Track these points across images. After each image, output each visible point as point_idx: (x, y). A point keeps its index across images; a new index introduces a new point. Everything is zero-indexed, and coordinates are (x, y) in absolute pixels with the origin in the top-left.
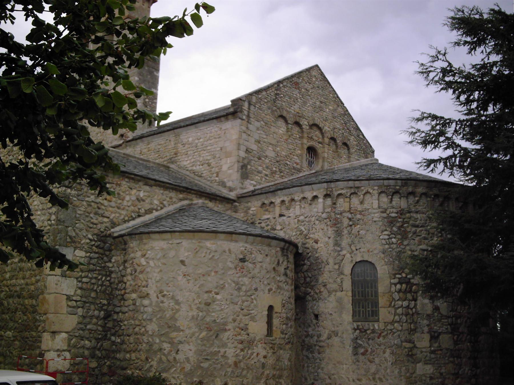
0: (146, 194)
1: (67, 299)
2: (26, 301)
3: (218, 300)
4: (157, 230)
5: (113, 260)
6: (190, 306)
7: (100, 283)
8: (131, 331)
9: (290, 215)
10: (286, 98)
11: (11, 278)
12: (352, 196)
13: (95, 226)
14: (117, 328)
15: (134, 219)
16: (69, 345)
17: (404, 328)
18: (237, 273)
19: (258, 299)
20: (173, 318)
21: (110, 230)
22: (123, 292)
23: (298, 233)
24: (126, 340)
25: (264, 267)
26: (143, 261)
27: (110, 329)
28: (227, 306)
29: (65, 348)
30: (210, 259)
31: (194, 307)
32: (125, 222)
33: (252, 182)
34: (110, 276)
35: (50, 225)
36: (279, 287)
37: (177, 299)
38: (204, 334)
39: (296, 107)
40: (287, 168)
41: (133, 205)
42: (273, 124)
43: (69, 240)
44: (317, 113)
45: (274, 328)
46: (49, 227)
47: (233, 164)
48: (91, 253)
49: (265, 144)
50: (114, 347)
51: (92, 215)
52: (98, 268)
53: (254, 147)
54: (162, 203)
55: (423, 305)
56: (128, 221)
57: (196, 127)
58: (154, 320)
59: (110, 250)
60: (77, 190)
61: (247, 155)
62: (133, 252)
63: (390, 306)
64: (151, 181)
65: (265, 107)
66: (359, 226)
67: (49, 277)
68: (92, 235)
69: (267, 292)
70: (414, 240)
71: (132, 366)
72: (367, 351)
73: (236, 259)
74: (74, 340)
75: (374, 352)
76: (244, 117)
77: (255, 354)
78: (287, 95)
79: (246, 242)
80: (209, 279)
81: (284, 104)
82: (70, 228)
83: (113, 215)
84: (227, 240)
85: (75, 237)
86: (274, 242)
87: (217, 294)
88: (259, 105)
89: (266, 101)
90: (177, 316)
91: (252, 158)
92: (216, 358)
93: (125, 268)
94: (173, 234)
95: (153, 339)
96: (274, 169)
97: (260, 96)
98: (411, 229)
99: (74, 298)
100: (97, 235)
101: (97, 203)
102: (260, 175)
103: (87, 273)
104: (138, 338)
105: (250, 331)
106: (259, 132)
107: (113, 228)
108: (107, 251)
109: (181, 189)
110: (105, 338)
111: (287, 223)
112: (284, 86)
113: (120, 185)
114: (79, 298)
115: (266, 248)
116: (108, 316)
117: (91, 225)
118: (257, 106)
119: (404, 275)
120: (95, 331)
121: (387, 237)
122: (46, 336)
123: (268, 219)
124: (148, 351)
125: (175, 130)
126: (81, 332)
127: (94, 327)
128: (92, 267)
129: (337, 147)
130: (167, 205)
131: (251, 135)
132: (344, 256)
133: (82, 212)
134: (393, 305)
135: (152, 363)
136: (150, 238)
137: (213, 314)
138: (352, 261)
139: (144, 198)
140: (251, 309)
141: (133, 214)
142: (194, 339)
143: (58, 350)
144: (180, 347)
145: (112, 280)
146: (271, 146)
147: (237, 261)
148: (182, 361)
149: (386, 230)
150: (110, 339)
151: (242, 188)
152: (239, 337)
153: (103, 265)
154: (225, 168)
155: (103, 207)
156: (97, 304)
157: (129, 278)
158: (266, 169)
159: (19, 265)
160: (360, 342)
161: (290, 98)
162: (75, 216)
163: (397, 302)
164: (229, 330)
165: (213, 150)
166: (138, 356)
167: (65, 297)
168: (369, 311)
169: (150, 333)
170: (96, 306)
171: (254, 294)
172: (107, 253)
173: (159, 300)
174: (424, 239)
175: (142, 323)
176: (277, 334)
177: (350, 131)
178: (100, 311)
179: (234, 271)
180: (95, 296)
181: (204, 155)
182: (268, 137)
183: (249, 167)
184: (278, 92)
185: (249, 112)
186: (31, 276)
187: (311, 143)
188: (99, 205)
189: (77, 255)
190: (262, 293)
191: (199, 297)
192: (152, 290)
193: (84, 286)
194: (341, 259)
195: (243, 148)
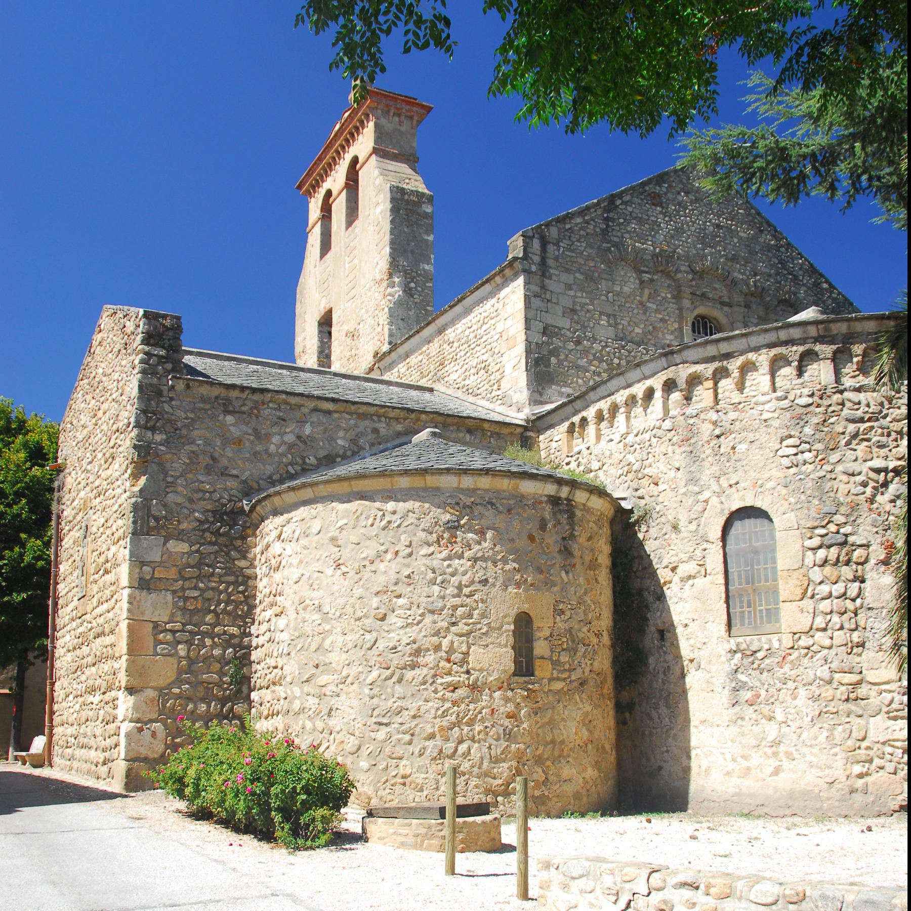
17: (836, 642)
23: (626, 469)
29: (154, 716)
30: (384, 529)
38: (375, 674)
42: (604, 276)
43: (153, 523)
48: (201, 544)
58: (293, 654)
66: (733, 436)
68: (203, 513)
70: (855, 450)
72: (758, 696)
75: (772, 696)
76: (534, 268)
88: (567, 242)
89: (582, 233)
92: (400, 721)
95: (291, 690)
96: (616, 361)
97: (568, 226)
98: (845, 428)
106: (572, 293)
112: (626, 203)
114: (178, 626)
118: (561, 244)
119: (832, 528)
121: (793, 451)
131: (554, 300)
132: (706, 501)
138: (723, 510)
149: (790, 436)
154: (508, 369)
160: (742, 677)
165: (489, 341)
167: (151, 625)
168: (761, 611)
169: (288, 679)
170: (216, 639)
172: (238, 543)
174: (879, 447)
176: (543, 670)
177: (794, 276)
184: (611, 215)
194: (700, 509)
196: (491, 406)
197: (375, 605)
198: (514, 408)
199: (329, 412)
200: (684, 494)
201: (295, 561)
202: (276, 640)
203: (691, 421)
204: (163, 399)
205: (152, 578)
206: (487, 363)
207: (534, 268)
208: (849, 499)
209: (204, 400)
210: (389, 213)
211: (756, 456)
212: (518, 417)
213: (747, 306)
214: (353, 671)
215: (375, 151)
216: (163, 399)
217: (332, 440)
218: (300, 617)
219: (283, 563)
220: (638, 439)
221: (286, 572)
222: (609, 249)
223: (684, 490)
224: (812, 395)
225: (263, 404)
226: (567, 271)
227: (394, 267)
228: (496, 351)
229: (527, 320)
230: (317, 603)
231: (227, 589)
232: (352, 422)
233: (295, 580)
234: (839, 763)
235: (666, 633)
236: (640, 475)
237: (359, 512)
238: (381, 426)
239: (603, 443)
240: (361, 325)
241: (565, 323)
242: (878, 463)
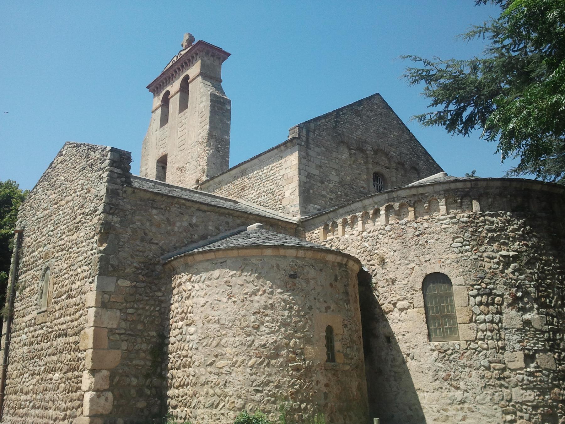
9: (353, 233)
12: (416, 205)
13: (141, 254)
15: (186, 245)
23: (363, 250)
29: (107, 387)
32: (176, 248)
33: (316, 206)
38: (253, 360)
39: (359, 133)
42: (334, 150)
43: (111, 269)
44: (381, 138)
53: (316, 172)
55: (512, 318)
61: (308, 180)
63: (471, 321)
66: (426, 235)
69: (323, 310)
75: (457, 376)
76: (303, 143)
81: (345, 130)
85: (118, 265)
88: (318, 131)
89: (325, 127)
92: (268, 388)
95: (199, 370)
96: (339, 193)
97: (319, 123)
98: (487, 234)
99: (117, 331)
102: (324, 199)
103: (132, 304)
106: (320, 157)
112: (343, 114)
114: (123, 331)
119: (484, 285)
121: (460, 245)
128: (138, 296)
129: (405, 171)
131: (312, 160)
132: (413, 269)
134: (474, 320)
141: (185, 240)
147: (287, 278)
149: (458, 237)
153: (151, 294)
154: (287, 194)
156: (145, 337)
159: (67, 301)
163: (478, 317)
167: (107, 330)
168: (446, 328)
169: (196, 363)
172: (156, 281)
181: (268, 185)
183: (311, 191)
184: (338, 119)
185: (307, 139)
187: (377, 169)
190: (317, 311)
194: (409, 272)
196: (276, 213)
197: (253, 320)
198: (291, 214)
199: (205, 211)
200: (400, 264)
201: (202, 293)
202: (187, 340)
203: (403, 227)
204: (119, 198)
205: (109, 301)
207: (303, 143)
208: (491, 271)
209: (141, 200)
210: (209, 108)
211: (439, 247)
212: (296, 219)
213: (397, 169)
214: (240, 359)
215: (201, 74)
216: (119, 198)
217: (206, 226)
218: (205, 327)
219: (193, 294)
220: (371, 235)
221: (195, 300)
222: (336, 136)
223: (399, 262)
224: (469, 217)
225: (172, 204)
226: (318, 146)
227: (210, 136)
228: (280, 184)
229: (299, 169)
230: (217, 318)
232: (217, 217)
233: (201, 304)
234: (499, 414)
235: (390, 338)
236: (372, 254)
237: (243, 267)
238: (230, 220)
239: (347, 236)
240: (187, 165)
241: (316, 172)
242: (504, 253)
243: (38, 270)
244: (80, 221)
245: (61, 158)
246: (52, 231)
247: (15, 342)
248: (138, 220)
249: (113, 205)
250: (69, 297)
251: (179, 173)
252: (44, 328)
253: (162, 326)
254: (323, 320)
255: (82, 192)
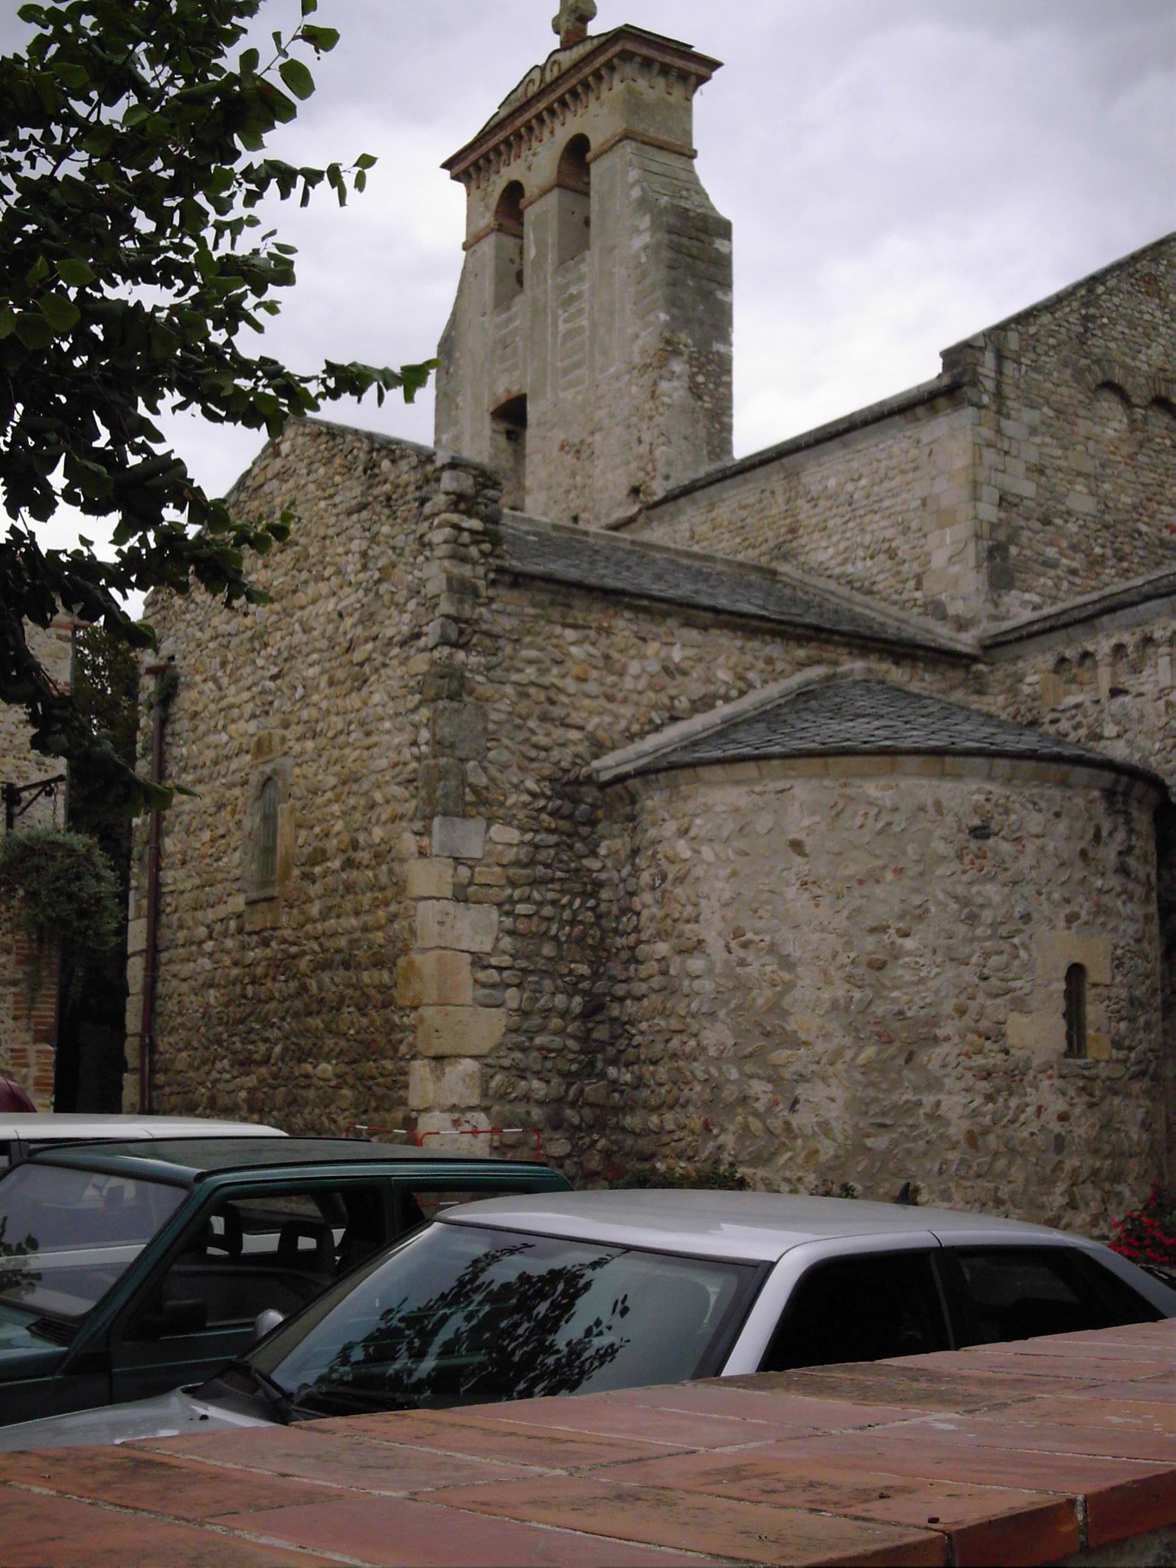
0: (690, 652)
1: (473, 964)
2: (366, 977)
3: (909, 953)
4: (718, 754)
5: (602, 851)
6: (825, 972)
7: (567, 915)
8: (659, 1047)
9: (1143, 689)
10: (1120, 328)
11: (324, 916)
13: (543, 754)
14: (622, 1043)
15: (657, 729)
16: (484, 1094)
18: (964, 872)
19: (1033, 946)
20: (776, 1008)
21: (588, 764)
22: (633, 937)
24: (647, 1075)
25: (1050, 848)
26: (683, 848)
27: (602, 1045)
28: (936, 970)
30: (880, 833)
31: (836, 975)
32: (631, 738)
33: (1027, 596)
34: (594, 894)
35: (418, 759)
36: (1100, 909)
37: (784, 953)
38: (870, 1051)
39: (1155, 351)
40: (1139, 543)
41: (651, 687)
42: (1082, 412)
43: (470, 797)
45: (1090, 1032)
46: (414, 765)
47: (961, 546)
48: (536, 831)
49: (1060, 475)
50: (616, 1095)
51: (532, 724)
52: (559, 874)
53: (1026, 488)
54: (742, 678)
56: (642, 734)
57: (845, 445)
58: (722, 1014)
59: (593, 823)
60: (484, 653)
61: (1003, 515)
62: (654, 824)
64: (702, 614)
65: (1051, 361)
67: (422, 905)
68: (538, 782)
71: (667, 1151)
73: (960, 830)
74: (498, 1078)
76: (986, 399)
77: (1030, 1110)
78: (1123, 316)
79: (990, 777)
80: (878, 891)
81: (1113, 345)
82: (472, 764)
83: (596, 720)
84: (931, 775)
85: (487, 788)
86: (1080, 774)
87: (906, 935)
88: (1032, 356)
89: (1052, 341)
90: (787, 1001)
91: (1023, 523)
92: (910, 1121)
93: (636, 871)
94: (763, 764)
95: (719, 1069)
96: (1098, 550)
97: (1032, 330)
99: (493, 961)
100: (551, 780)
101: (545, 688)
102: (1052, 573)
103: (527, 890)
104: (679, 1070)
105: (1012, 1040)
106: (1038, 440)
107: (596, 757)
108: (584, 824)
109: (800, 631)
110: (588, 1071)
111: (1135, 714)
112: (1110, 292)
113: (608, 632)
114: (506, 961)
115: (1056, 793)
116: (594, 1009)
117: (533, 753)
118: (1023, 360)
120: (559, 1051)
122: (420, 1069)
123: (1077, 706)
124: (708, 1104)
125: (785, 460)
126: (518, 1055)
127: (557, 1042)
128: (540, 870)
130: (758, 685)
131: (1014, 452)
133: (504, 717)
135: (722, 1139)
136: (698, 780)
137: (895, 994)
139: (685, 665)
140: (1010, 976)
142: (840, 1066)
143: (453, 1108)
144: (800, 1090)
145: (603, 907)
146: (1080, 479)
148: (808, 1131)
150: (603, 1075)
151: (995, 618)
152: (979, 1061)
153: (573, 865)
154: (939, 559)
155: (563, 698)
156: (562, 976)
157: (647, 897)
158: (1071, 554)
159: (344, 875)
161: (1132, 326)
162: (485, 730)
164: (947, 1039)
165: (899, 508)
166: (684, 1121)
167: (468, 958)
169: (712, 1052)
170: (559, 982)
171: (1019, 931)
172: (585, 830)
173: (733, 957)
175: (688, 1026)
176: (1099, 1048)
178: (571, 996)
179: (955, 866)
180: (553, 954)
181: (876, 526)
182: (1069, 453)
183: (1013, 550)
185: (999, 384)
186: (376, 904)
188: (552, 694)
189: (497, 839)
190: (1045, 927)
191: (849, 945)
192: (711, 931)
193: (521, 926)
195: (990, 494)
204: (481, 601)
206: (894, 544)
226: (1032, 406)
231: (571, 903)
240: (598, 437)
243: (233, 785)
244: (368, 659)
245: (277, 464)
246: (273, 678)
247: (175, 976)
248: (530, 662)
249: (466, 621)
250: (349, 864)
251: (569, 459)
252: (273, 944)
253: (605, 950)
254: (1055, 947)
255: (362, 576)
